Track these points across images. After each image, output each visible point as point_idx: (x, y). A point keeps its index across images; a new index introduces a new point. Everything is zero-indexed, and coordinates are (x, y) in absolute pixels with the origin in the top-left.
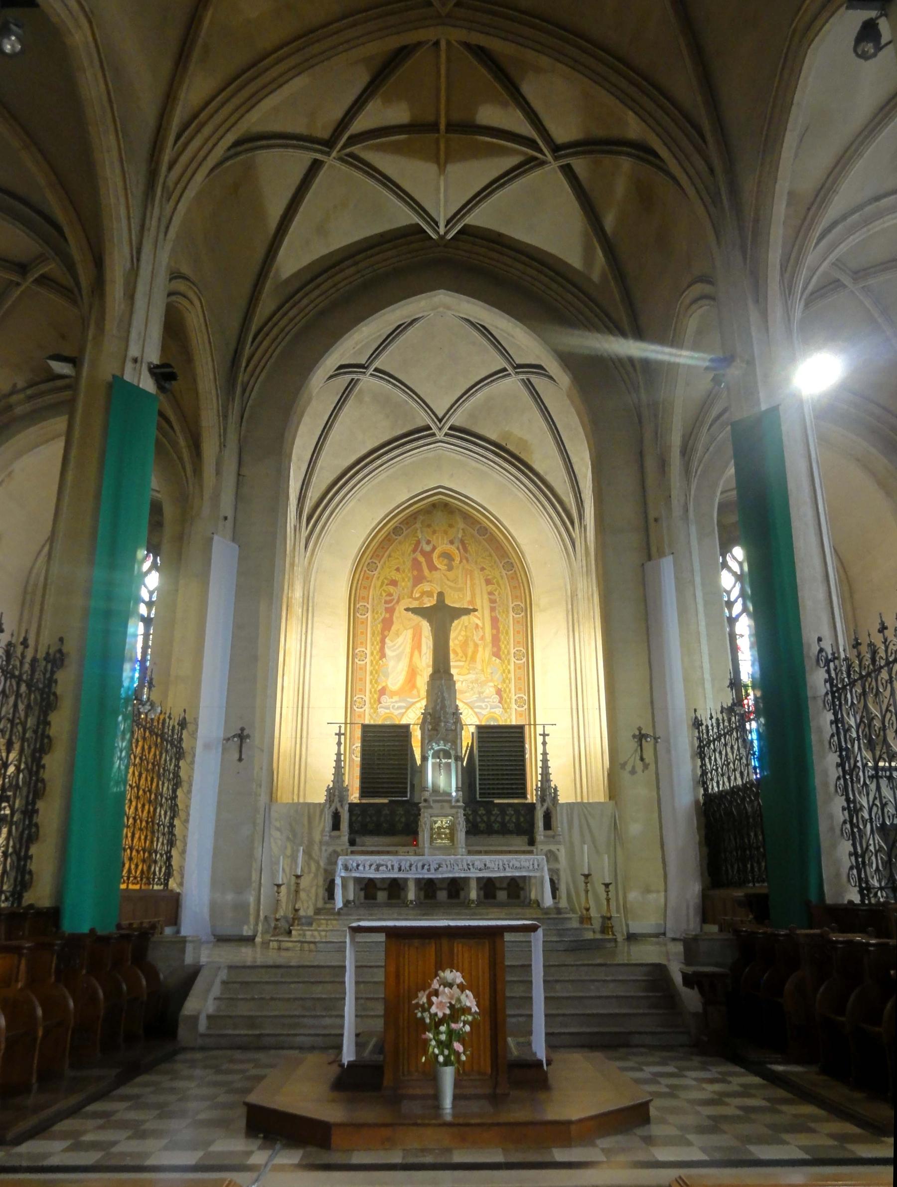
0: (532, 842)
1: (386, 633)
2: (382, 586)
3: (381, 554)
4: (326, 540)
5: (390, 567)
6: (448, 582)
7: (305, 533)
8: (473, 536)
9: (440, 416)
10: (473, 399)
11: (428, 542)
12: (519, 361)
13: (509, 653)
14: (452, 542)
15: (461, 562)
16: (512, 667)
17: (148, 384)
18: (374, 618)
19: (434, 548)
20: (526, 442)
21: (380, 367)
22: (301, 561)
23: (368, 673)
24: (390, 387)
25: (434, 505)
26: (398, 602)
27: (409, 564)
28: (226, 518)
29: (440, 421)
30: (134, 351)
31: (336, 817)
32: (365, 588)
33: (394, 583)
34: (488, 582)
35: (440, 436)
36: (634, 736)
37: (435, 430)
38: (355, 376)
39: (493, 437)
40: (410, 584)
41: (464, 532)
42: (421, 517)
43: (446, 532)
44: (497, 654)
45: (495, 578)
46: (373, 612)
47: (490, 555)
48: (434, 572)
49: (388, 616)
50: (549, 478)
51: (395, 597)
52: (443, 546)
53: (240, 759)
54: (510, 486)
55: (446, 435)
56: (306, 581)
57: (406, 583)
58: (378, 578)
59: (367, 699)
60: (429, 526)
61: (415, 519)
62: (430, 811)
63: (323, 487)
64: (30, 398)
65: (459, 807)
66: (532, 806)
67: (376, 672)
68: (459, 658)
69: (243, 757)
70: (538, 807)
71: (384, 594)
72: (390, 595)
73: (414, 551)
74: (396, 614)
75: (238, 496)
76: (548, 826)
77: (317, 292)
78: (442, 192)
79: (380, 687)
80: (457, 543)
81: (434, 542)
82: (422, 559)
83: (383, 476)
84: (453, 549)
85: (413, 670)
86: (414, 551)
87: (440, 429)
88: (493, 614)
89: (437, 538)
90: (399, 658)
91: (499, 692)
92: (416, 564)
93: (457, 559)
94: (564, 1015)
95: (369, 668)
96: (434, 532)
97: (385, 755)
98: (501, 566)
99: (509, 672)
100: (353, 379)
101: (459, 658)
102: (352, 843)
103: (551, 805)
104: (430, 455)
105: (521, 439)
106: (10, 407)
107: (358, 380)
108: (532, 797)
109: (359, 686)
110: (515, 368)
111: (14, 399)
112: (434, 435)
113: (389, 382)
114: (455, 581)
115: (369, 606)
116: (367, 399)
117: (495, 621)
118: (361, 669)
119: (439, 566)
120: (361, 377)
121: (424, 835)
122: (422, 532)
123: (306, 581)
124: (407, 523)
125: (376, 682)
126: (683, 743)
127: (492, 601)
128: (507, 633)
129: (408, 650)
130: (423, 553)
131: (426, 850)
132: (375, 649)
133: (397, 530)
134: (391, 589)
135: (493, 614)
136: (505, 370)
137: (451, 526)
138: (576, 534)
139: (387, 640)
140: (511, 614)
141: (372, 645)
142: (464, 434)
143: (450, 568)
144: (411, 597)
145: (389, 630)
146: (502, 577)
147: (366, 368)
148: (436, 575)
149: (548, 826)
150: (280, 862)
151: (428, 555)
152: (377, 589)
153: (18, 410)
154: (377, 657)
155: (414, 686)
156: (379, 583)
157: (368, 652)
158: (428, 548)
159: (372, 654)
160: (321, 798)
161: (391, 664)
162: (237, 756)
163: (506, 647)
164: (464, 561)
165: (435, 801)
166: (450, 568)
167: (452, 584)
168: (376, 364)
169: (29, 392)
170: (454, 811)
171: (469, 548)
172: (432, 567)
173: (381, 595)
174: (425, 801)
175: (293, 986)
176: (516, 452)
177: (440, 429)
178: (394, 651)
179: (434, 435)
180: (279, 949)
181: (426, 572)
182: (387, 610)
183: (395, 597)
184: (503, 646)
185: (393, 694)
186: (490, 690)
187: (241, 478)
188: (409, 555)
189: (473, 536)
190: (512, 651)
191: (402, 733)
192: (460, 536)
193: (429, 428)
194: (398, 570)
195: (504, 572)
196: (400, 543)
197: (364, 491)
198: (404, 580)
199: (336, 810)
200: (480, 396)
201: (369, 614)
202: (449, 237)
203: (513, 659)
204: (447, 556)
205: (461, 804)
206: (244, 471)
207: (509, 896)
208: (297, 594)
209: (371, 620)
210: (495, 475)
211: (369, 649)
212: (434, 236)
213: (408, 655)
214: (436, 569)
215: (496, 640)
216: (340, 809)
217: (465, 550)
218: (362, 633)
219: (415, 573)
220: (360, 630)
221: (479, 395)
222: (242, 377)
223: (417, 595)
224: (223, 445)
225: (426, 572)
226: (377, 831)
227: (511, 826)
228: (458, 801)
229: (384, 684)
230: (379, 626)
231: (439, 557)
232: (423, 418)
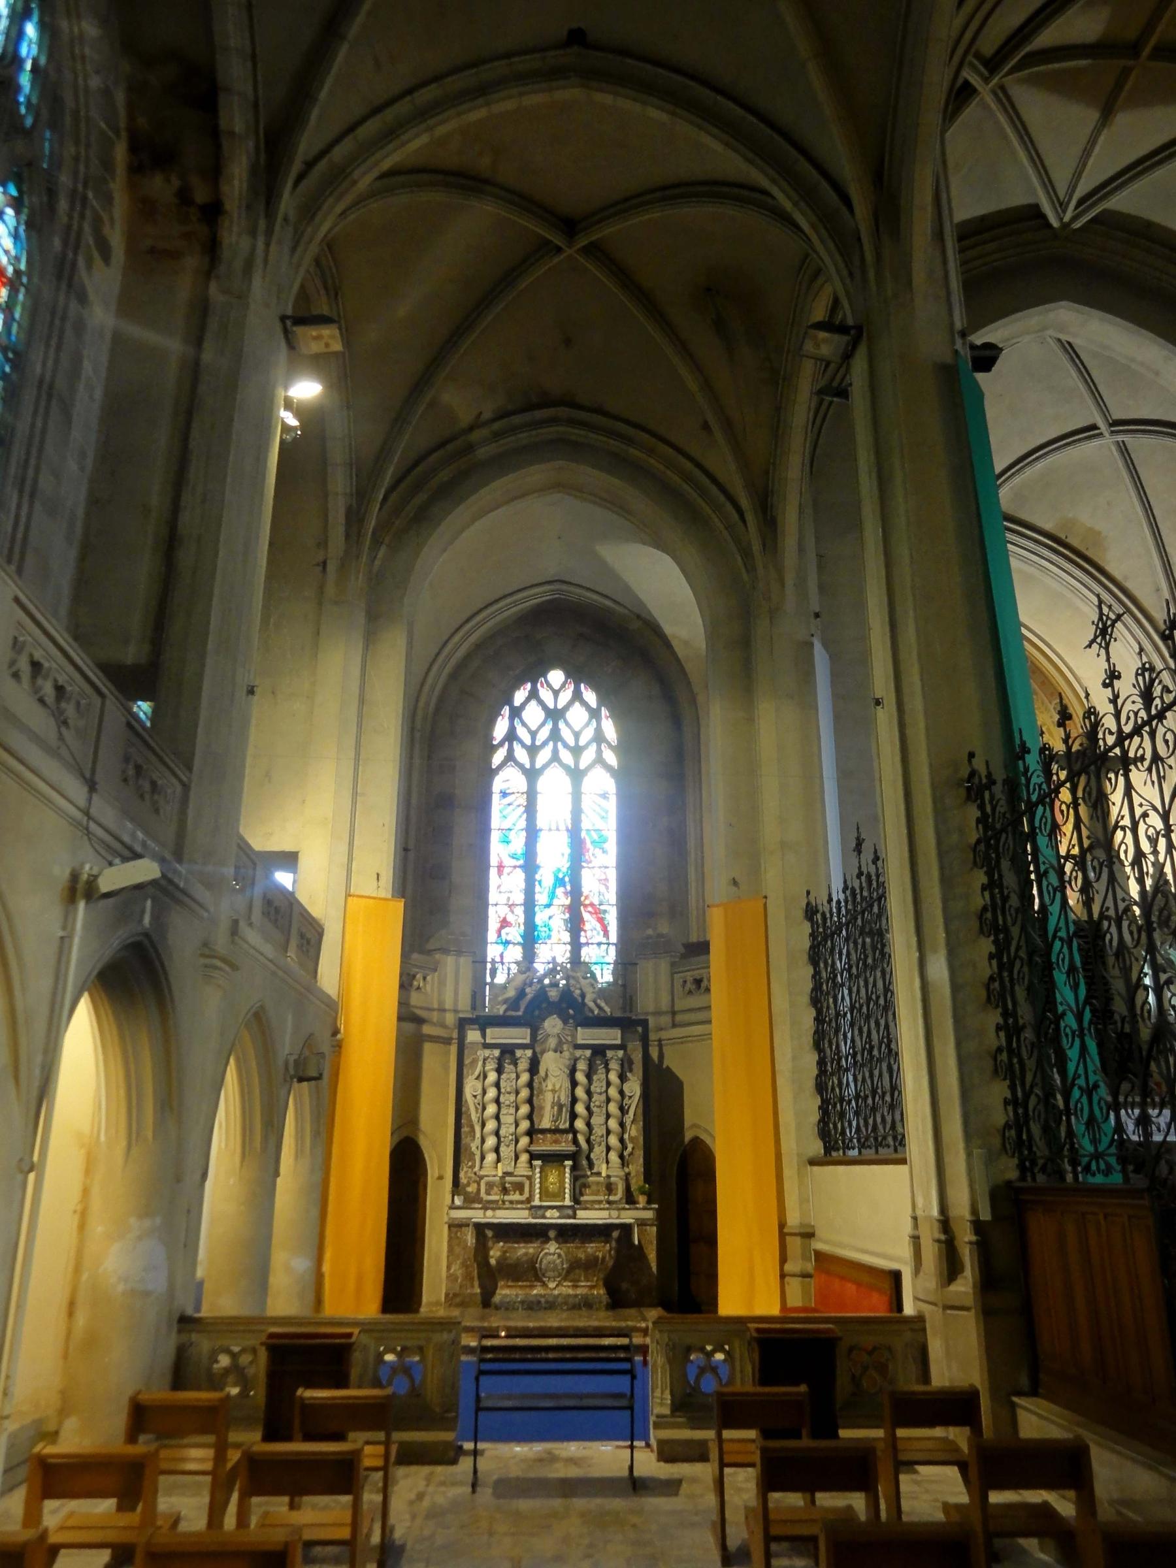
10: (1029, 472)
12: (1117, 415)
39: (1048, 526)
54: (1069, 595)
64: (497, 435)
105: (1091, 529)
106: (470, 448)
110: (1111, 425)
111: (475, 436)
136: (1094, 427)
153: (483, 452)
169: (496, 426)
176: (1082, 548)
202: (1077, 225)
210: (1048, 581)
212: (1055, 223)
221: (1039, 466)
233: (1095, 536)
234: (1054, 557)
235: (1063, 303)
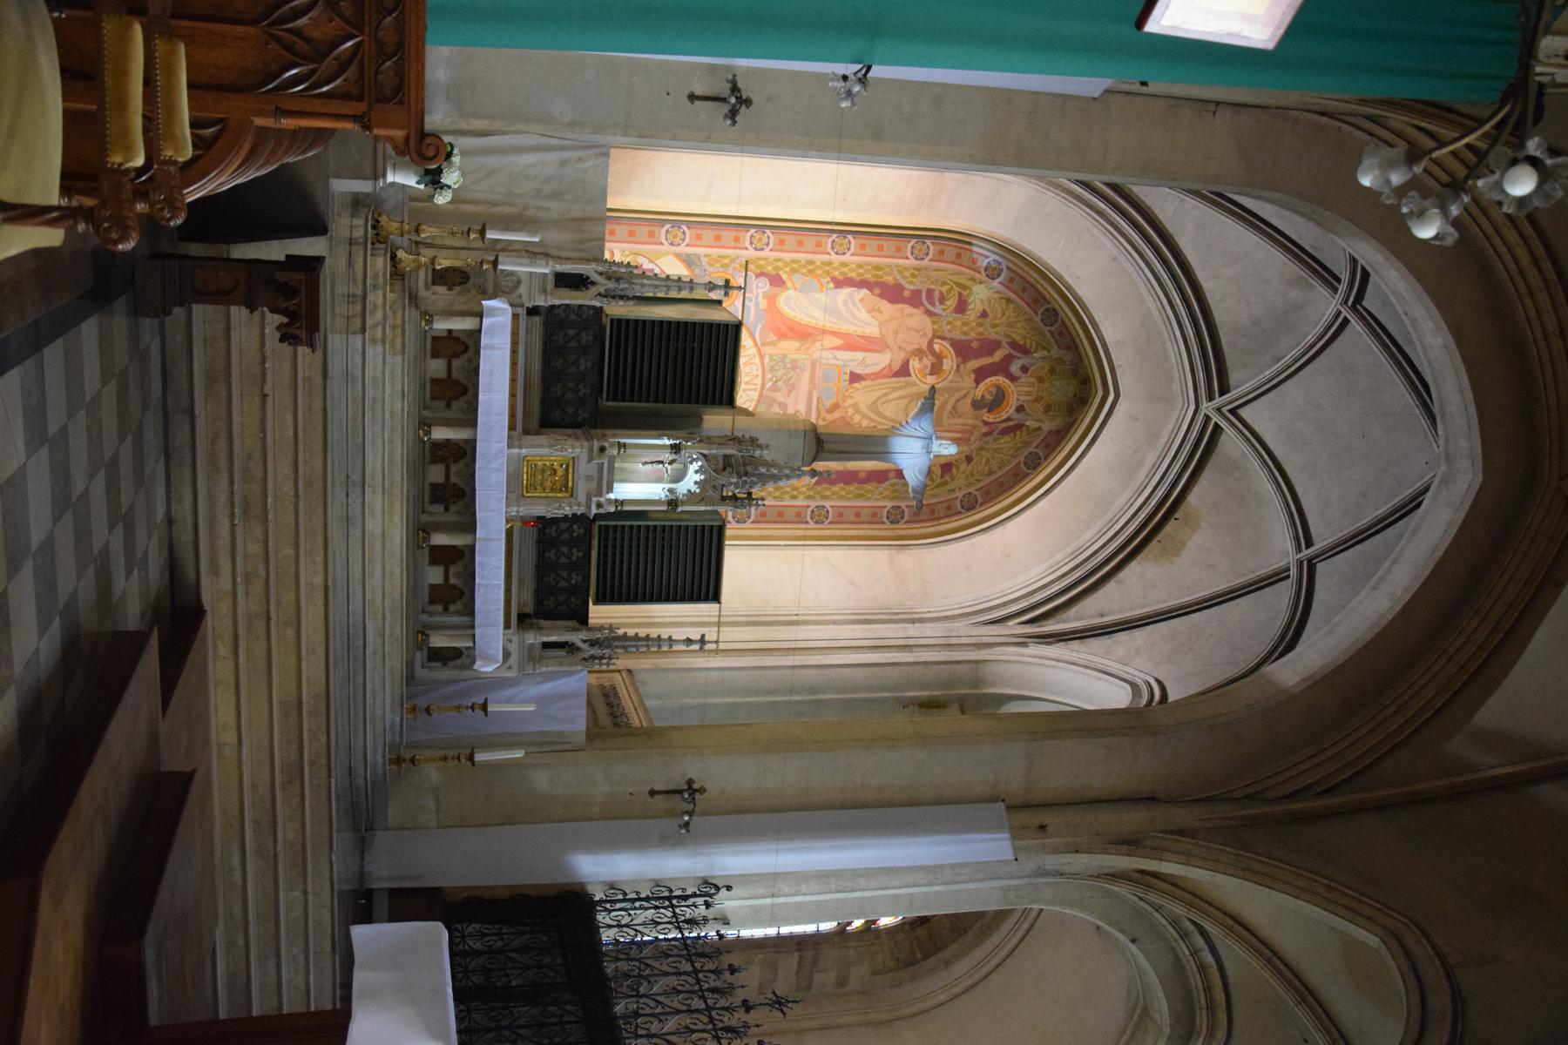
1: (877, 291)
2: (958, 285)
3: (1015, 286)
5: (989, 301)
6: (952, 401)
8: (1026, 444)
9: (1242, 412)
10: (1262, 474)
11: (1024, 369)
12: (1321, 568)
13: (825, 498)
14: (1020, 409)
15: (986, 423)
16: (800, 502)
18: (906, 269)
19: (1013, 378)
20: (1177, 555)
21: (1348, 329)
23: (809, 257)
24: (1310, 338)
25: (1086, 381)
26: (929, 313)
27: (992, 334)
28: (1144, 84)
29: (1232, 411)
32: (959, 255)
33: (961, 307)
35: (1207, 407)
36: (690, 782)
37: (1218, 401)
38: (1342, 288)
39: (1192, 498)
40: (957, 335)
41: (1036, 430)
42: (1068, 357)
43: (1038, 399)
45: (953, 479)
46: (918, 269)
47: (991, 473)
48: (973, 376)
49: (907, 294)
51: (938, 309)
52: (1016, 394)
53: (692, 97)
54: (1106, 518)
55: (1208, 418)
57: (959, 328)
58: (973, 279)
59: (766, 253)
60: (1052, 371)
61: (1068, 348)
62: (584, 456)
65: (589, 507)
66: (582, 618)
67: (811, 270)
68: (824, 414)
69: (697, 103)
70: (584, 635)
71: (944, 289)
72: (942, 300)
73: (1013, 345)
74: (908, 309)
77: (1525, 260)
79: (784, 277)
80: (1018, 418)
81: (1024, 379)
82: (998, 356)
83: (1152, 305)
84: (1009, 410)
85: (810, 335)
86: (1013, 345)
87: (1219, 410)
88: (892, 475)
89: (1029, 385)
90: (830, 310)
92: (989, 347)
93: (990, 418)
94: (247, 945)
95: (819, 258)
96: (1041, 380)
98: (972, 490)
99: (794, 497)
100: (1339, 281)
101: (824, 414)
102: (533, 311)
103: (586, 656)
104: (1176, 387)
105: (1183, 545)
107: (1336, 290)
108: (600, 614)
109: (791, 239)
110: (1310, 561)
112: (1211, 398)
113: (1320, 339)
114: (955, 412)
115: (926, 262)
116: (1294, 294)
118: (819, 244)
119: (982, 386)
120: (1339, 296)
122: (1044, 358)
124: (1061, 334)
125: (794, 271)
126: (676, 865)
128: (859, 496)
129: (845, 328)
130: (1008, 359)
131: (515, 451)
132: (852, 270)
133: (1051, 315)
134: (952, 302)
135: (892, 475)
136: (1309, 544)
137: (1048, 409)
138: (1013, 627)
139: (864, 292)
140: (889, 504)
141: (859, 266)
142: (1202, 450)
143: (977, 405)
144: (934, 336)
145: (881, 296)
146: (952, 491)
147: (1353, 307)
148: (968, 382)
151: (1002, 368)
152: (955, 278)
154: (836, 273)
155: (782, 336)
156: (963, 281)
157: (847, 258)
158: (1015, 368)
159: (844, 264)
161: (822, 298)
162: (699, 91)
163: (834, 493)
164: (985, 429)
165: (601, 467)
166: (977, 405)
167: (949, 408)
168: (1354, 323)
170: (582, 498)
171: (1007, 438)
172: (980, 375)
173: (944, 283)
174: (602, 449)
175: (289, 418)
177: (1219, 410)
178: (845, 303)
179: (1211, 398)
180: (352, 242)
181: (975, 364)
182: (917, 293)
183: (938, 309)
184: (836, 488)
185: (771, 299)
187: (1212, 107)
188: (1007, 336)
189: (1026, 444)
190: (827, 504)
191: (722, 391)
192: (1028, 423)
193: (1224, 390)
194: (984, 314)
195: (960, 494)
196: (1030, 320)
197: (1130, 269)
198: (965, 324)
199: (593, 283)
200: (1265, 486)
201: (912, 262)
203: (813, 504)
204: (998, 400)
205: (594, 511)
206: (1224, 114)
207: (433, 587)
209: (899, 265)
210: (1128, 494)
211: (853, 259)
213: (835, 328)
214: (978, 381)
216: (594, 290)
217: (1004, 432)
218: (881, 248)
219: (975, 345)
220: (889, 245)
221: (1269, 487)
223: (936, 347)
225: (975, 364)
227: (551, 579)
228: (599, 505)
229: (789, 284)
230: (889, 279)
231: (998, 387)
232: (1242, 381)
233: (1175, 550)
234: (1154, 502)
235: (1481, 477)
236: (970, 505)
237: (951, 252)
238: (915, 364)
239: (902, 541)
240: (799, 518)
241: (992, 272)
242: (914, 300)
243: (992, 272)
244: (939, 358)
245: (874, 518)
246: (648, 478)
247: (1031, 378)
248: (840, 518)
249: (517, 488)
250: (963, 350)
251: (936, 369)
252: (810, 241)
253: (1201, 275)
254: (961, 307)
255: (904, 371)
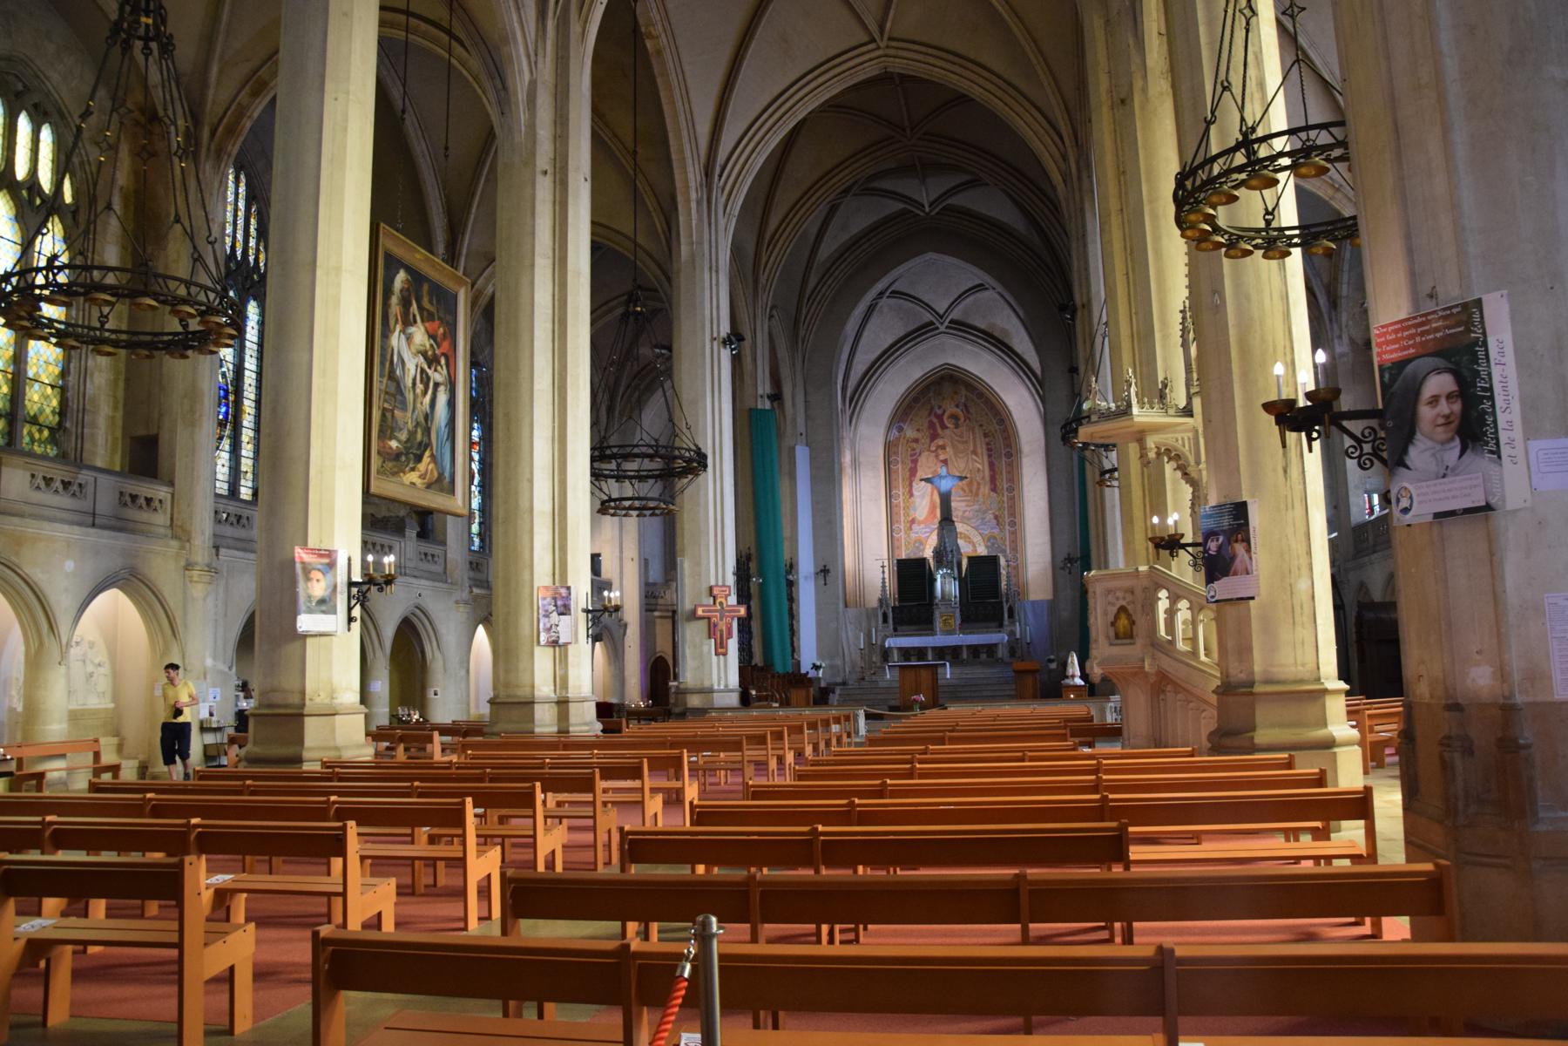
0: (1001, 625)
4: (865, 415)
7: (848, 413)
17: (768, 405)
22: (847, 434)
25: (942, 378)
30: (760, 392)
31: (885, 616)
34: (986, 435)
35: (942, 329)
39: (983, 327)
44: (994, 489)
50: (1025, 357)
52: (951, 409)
56: (853, 448)
63: (859, 375)
67: (906, 508)
75: (807, 417)
76: (1011, 615)
78: (925, 193)
90: (923, 496)
91: (996, 517)
92: (932, 426)
97: (912, 575)
102: (895, 630)
117: (992, 465)
121: (938, 624)
123: (853, 448)
127: (989, 450)
133: (916, 400)
142: (962, 328)
143: (957, 426)
148: (947, 432)
149: (1011, 615)
150: (854, 640)
151: (940, 418)
158: (939, 412)
160: (875, 604)
172: (944, 427)
186: (990, 516)
191: (922, 562)
204: (954, 417)
208: (847, 459)
209: (901, 470)
211: (900, 491)
215: (993, 479)
222: (802, 333)
224: (794, 386)
226: (910, 623)
232: (928, 317)
236: (1001, 421)
237: (893, 449)
238: (942, 457)
239: (1019, 451)
240: (1012, 498)
241: (900, 430)
242: (915, 462)
243: (900, 430)
244: (939, 447)
245: (1010, 465)
246: (945, 585)
247: (948, 404)
248: (1011, 480)
249: (950, 633)
250: (934, 437)
251: (943, 447)
252: (895, 510)
253: (886, 346)
254: (916, 441)
255: (945, 462)
